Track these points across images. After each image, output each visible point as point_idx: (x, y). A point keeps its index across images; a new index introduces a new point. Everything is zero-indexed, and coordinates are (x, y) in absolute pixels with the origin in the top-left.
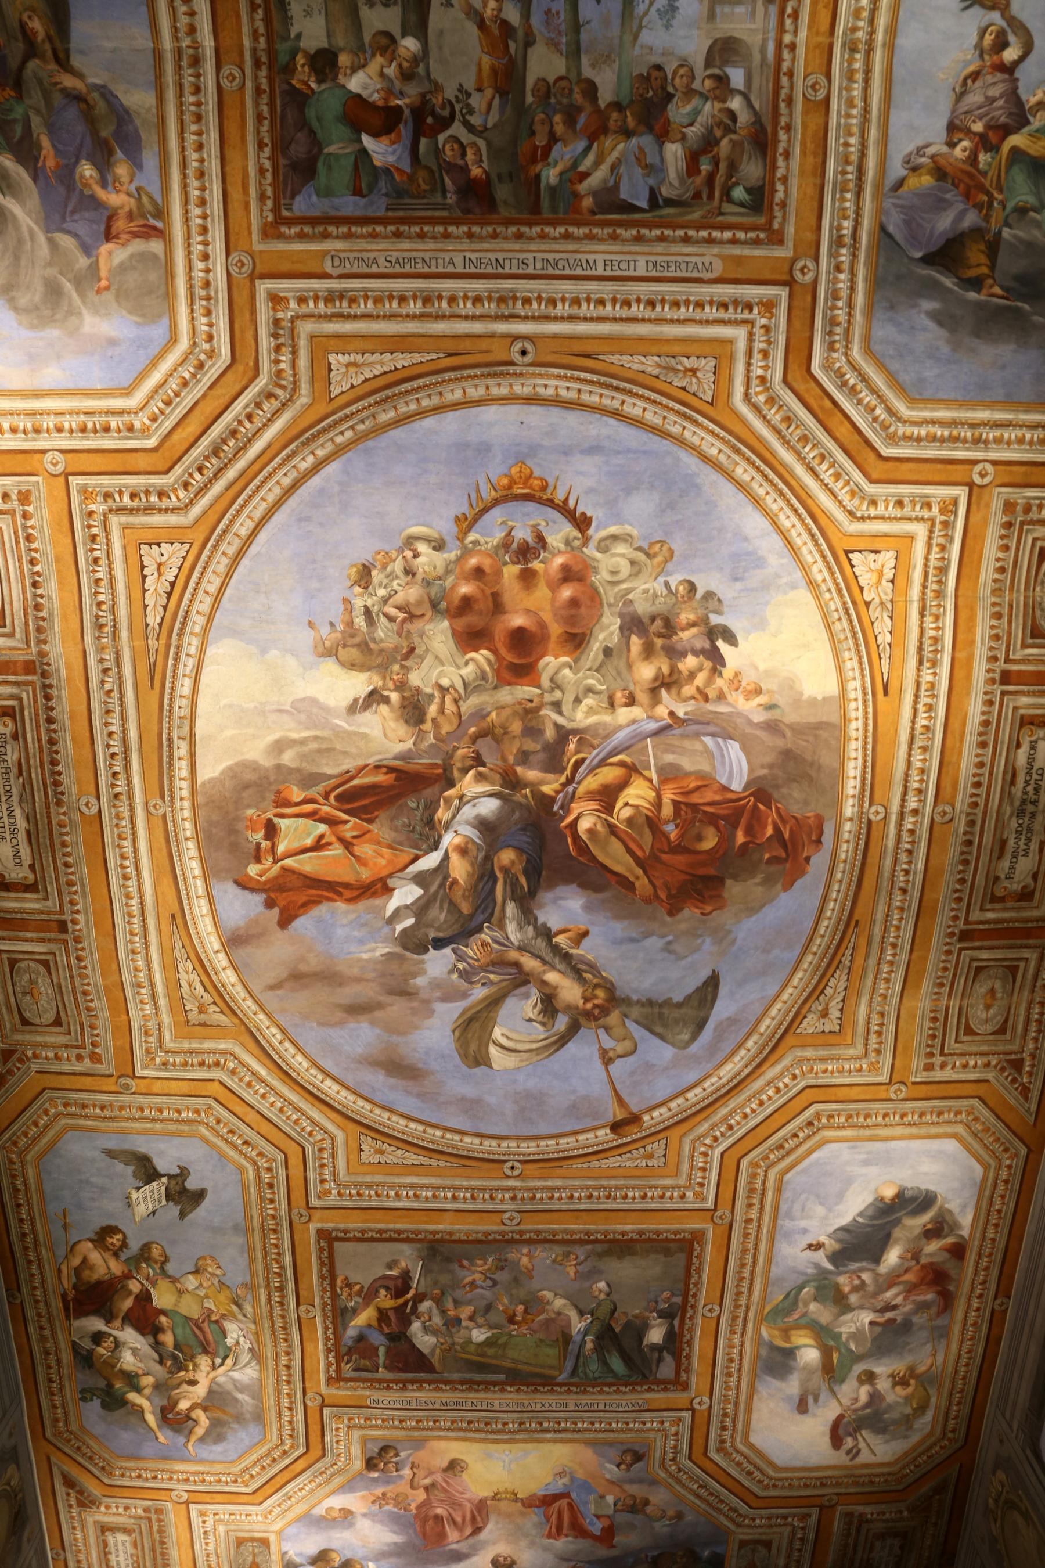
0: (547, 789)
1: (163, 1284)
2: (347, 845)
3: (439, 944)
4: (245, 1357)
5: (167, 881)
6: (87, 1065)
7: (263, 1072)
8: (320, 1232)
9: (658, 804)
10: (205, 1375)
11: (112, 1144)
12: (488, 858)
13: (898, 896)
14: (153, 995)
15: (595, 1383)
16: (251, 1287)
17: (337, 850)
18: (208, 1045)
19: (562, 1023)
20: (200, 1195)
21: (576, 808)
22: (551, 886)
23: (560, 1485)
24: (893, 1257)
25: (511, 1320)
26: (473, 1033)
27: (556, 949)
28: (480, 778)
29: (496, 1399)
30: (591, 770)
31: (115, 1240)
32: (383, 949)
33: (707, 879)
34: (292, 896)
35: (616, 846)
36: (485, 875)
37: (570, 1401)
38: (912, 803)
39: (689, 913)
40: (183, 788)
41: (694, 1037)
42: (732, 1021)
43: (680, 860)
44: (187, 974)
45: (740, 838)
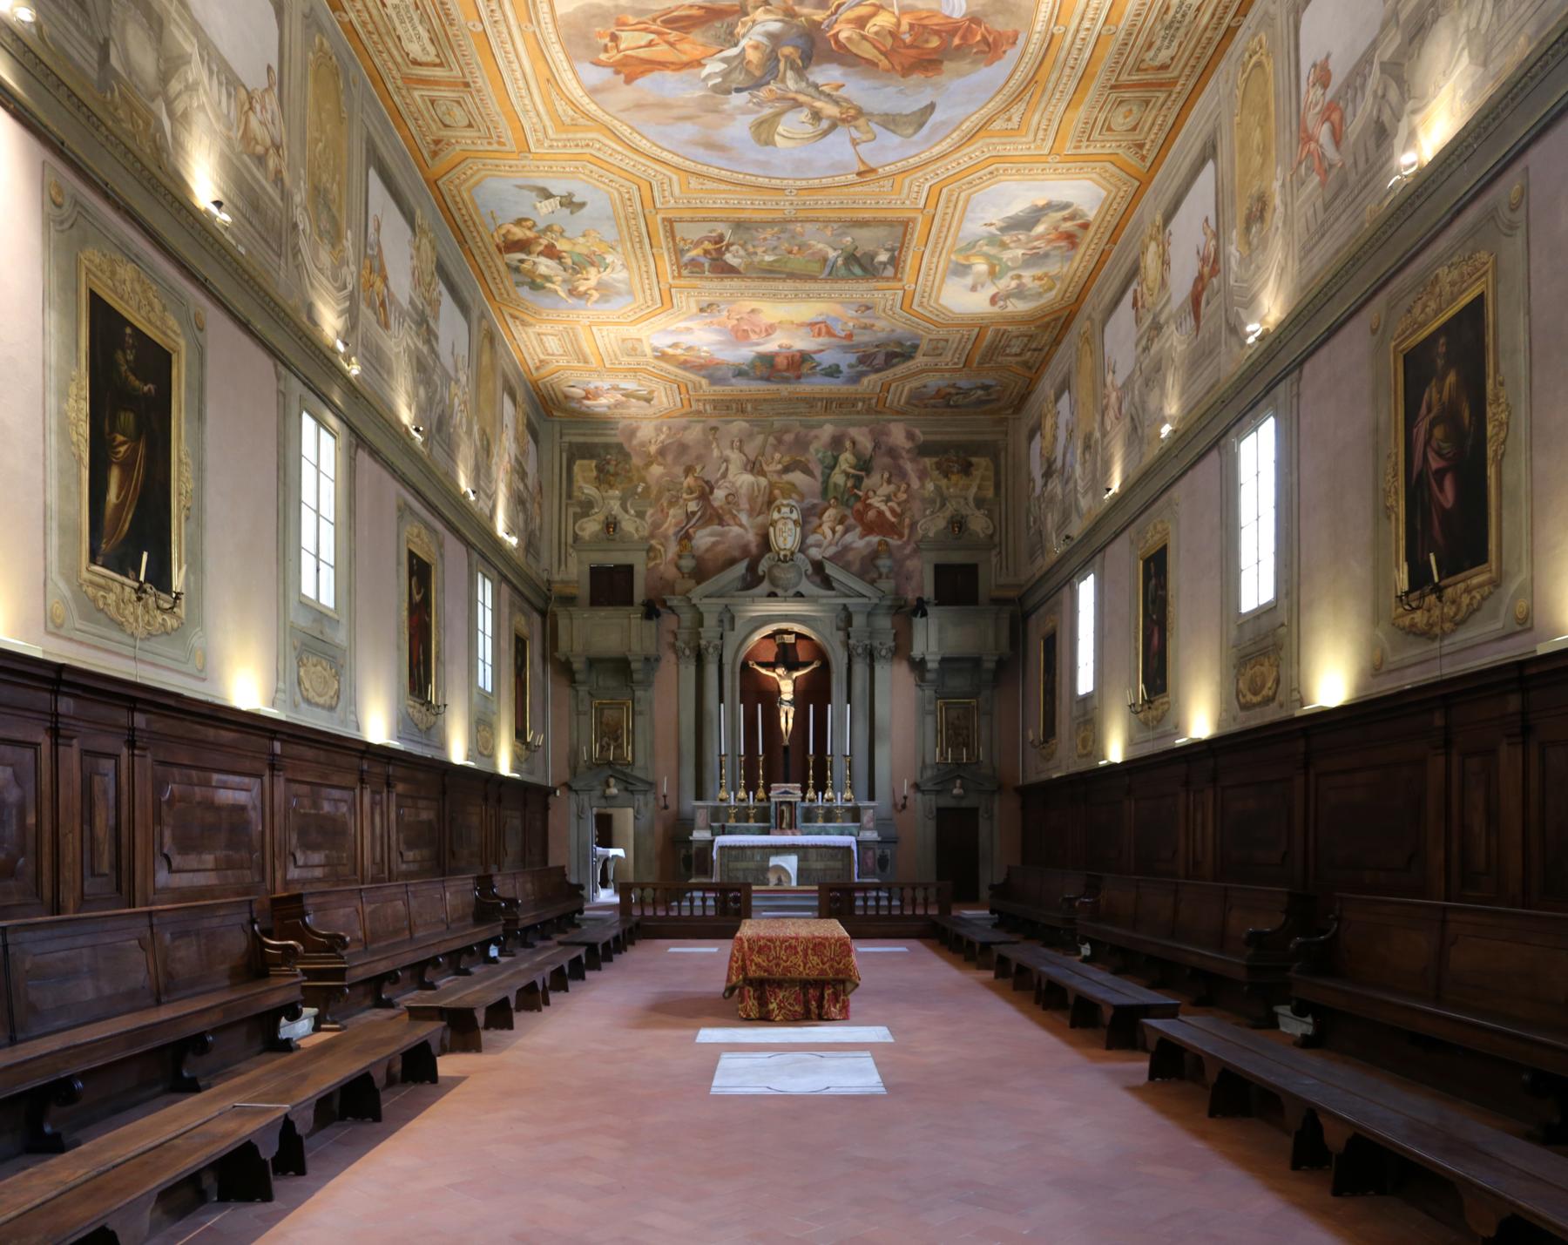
0: (816, 18)
1: (563, 241)
2: (671, 44)
3: (738, 90)
4: (619, 268)
5: (541, 64)
6: (495, 147)
7: (620, 149)
8: (664, 220)
9: (898, 24)
10: (593, 276)
11: (520, 182)
12: (773, 51)
13: (1067, 71)
14: (538, 115)
15: (843, 279)
16: (621, 241)
17: (665, 47)
18: (579, 135)
19: (825, 124)
20: (582, 205)
21: (837, 28)
22: (818, 64)
23: (820, 319)
24: (1040, 229)
25: (790, 252)
26: (764, 131)
27: (822, 93)
28: (768, 11)
29: (780, 285)
30: (850, 8)
31: (529, 223)
32: (698, 93)
33: (932, 62)
34: (631, 69)
35: (866, 45)
36: (771, 59)
37: (828, 286)
38: (1086, 24)
39: (916, 77)
40: (545, 17)
41: (915, 132)
42: (943, 123)
43: (913, 52)
44: (561, 107)
45: (957, 41)
